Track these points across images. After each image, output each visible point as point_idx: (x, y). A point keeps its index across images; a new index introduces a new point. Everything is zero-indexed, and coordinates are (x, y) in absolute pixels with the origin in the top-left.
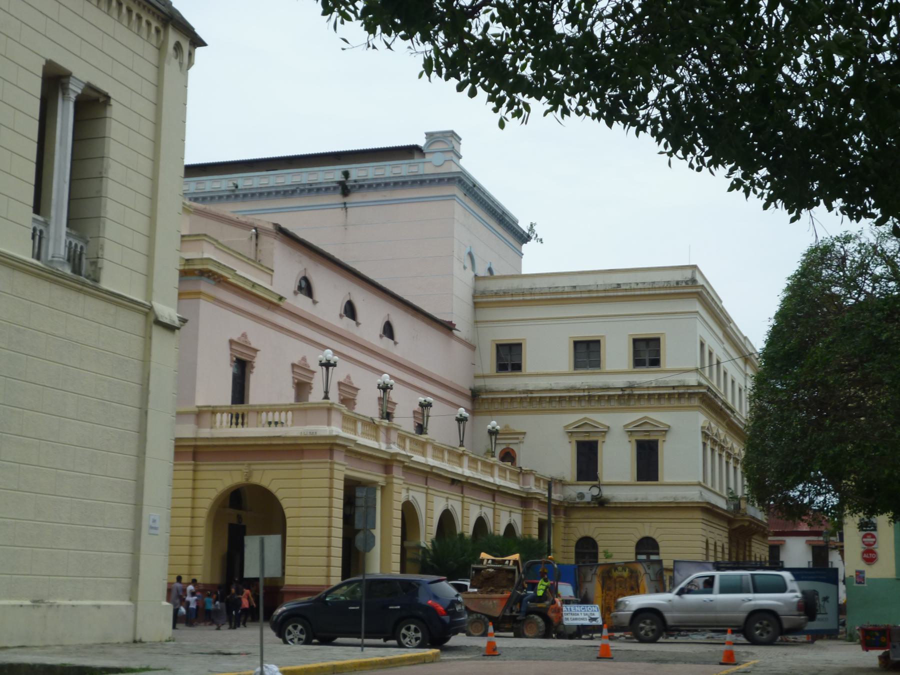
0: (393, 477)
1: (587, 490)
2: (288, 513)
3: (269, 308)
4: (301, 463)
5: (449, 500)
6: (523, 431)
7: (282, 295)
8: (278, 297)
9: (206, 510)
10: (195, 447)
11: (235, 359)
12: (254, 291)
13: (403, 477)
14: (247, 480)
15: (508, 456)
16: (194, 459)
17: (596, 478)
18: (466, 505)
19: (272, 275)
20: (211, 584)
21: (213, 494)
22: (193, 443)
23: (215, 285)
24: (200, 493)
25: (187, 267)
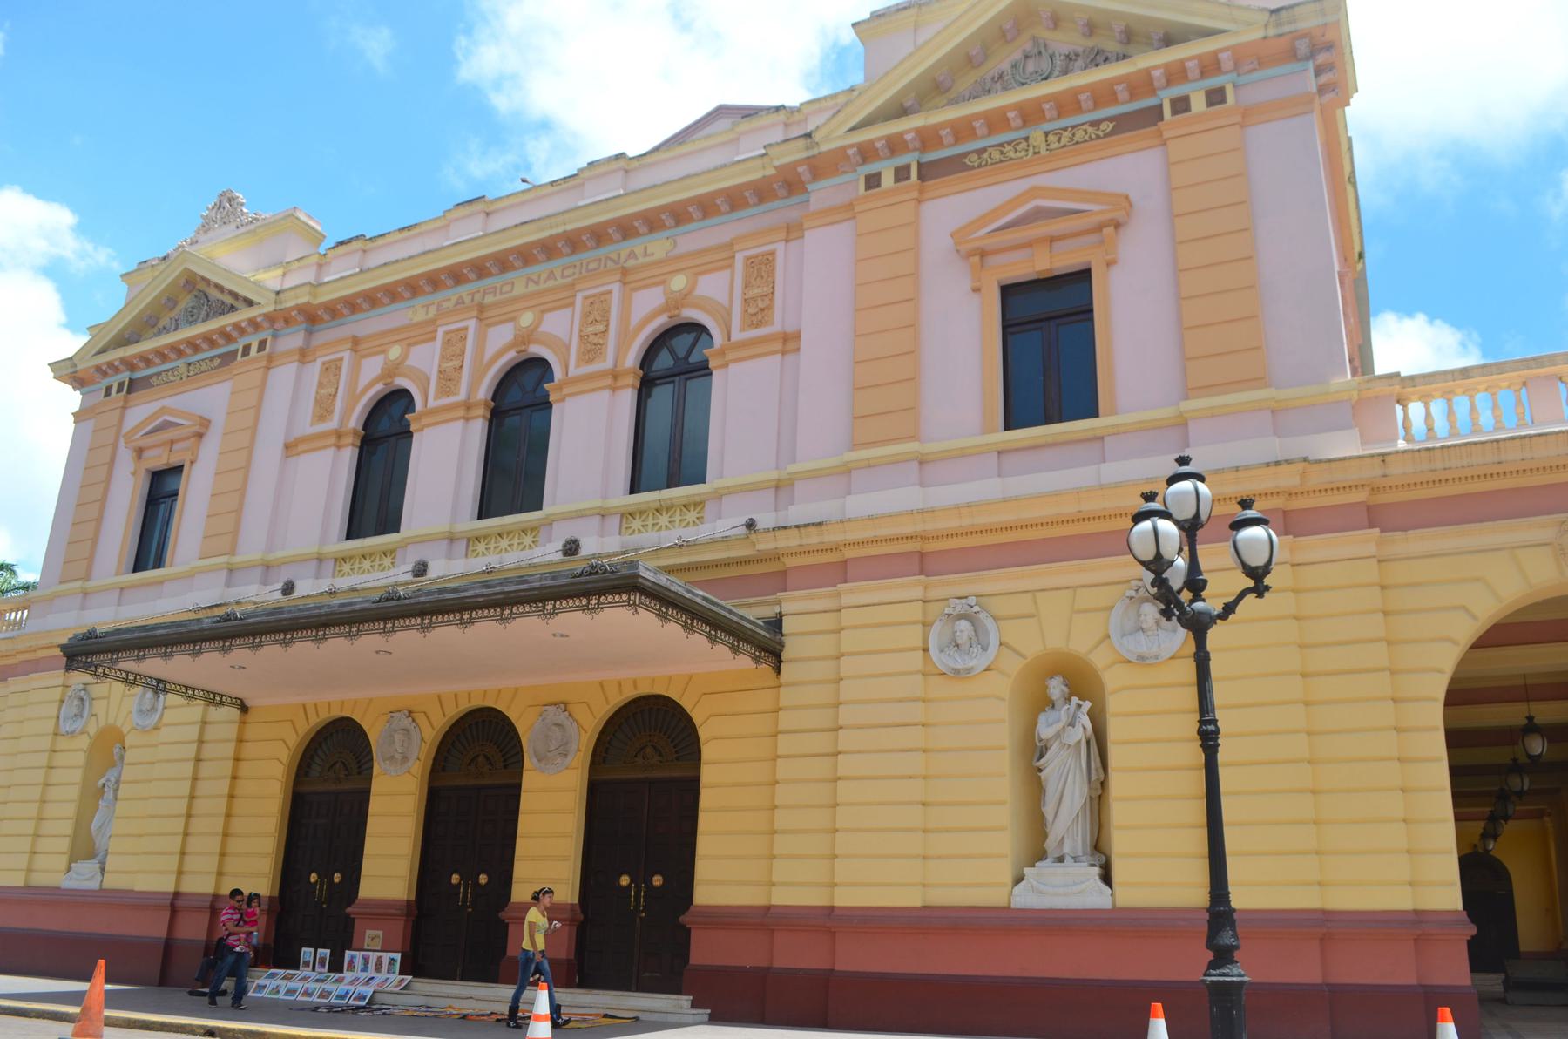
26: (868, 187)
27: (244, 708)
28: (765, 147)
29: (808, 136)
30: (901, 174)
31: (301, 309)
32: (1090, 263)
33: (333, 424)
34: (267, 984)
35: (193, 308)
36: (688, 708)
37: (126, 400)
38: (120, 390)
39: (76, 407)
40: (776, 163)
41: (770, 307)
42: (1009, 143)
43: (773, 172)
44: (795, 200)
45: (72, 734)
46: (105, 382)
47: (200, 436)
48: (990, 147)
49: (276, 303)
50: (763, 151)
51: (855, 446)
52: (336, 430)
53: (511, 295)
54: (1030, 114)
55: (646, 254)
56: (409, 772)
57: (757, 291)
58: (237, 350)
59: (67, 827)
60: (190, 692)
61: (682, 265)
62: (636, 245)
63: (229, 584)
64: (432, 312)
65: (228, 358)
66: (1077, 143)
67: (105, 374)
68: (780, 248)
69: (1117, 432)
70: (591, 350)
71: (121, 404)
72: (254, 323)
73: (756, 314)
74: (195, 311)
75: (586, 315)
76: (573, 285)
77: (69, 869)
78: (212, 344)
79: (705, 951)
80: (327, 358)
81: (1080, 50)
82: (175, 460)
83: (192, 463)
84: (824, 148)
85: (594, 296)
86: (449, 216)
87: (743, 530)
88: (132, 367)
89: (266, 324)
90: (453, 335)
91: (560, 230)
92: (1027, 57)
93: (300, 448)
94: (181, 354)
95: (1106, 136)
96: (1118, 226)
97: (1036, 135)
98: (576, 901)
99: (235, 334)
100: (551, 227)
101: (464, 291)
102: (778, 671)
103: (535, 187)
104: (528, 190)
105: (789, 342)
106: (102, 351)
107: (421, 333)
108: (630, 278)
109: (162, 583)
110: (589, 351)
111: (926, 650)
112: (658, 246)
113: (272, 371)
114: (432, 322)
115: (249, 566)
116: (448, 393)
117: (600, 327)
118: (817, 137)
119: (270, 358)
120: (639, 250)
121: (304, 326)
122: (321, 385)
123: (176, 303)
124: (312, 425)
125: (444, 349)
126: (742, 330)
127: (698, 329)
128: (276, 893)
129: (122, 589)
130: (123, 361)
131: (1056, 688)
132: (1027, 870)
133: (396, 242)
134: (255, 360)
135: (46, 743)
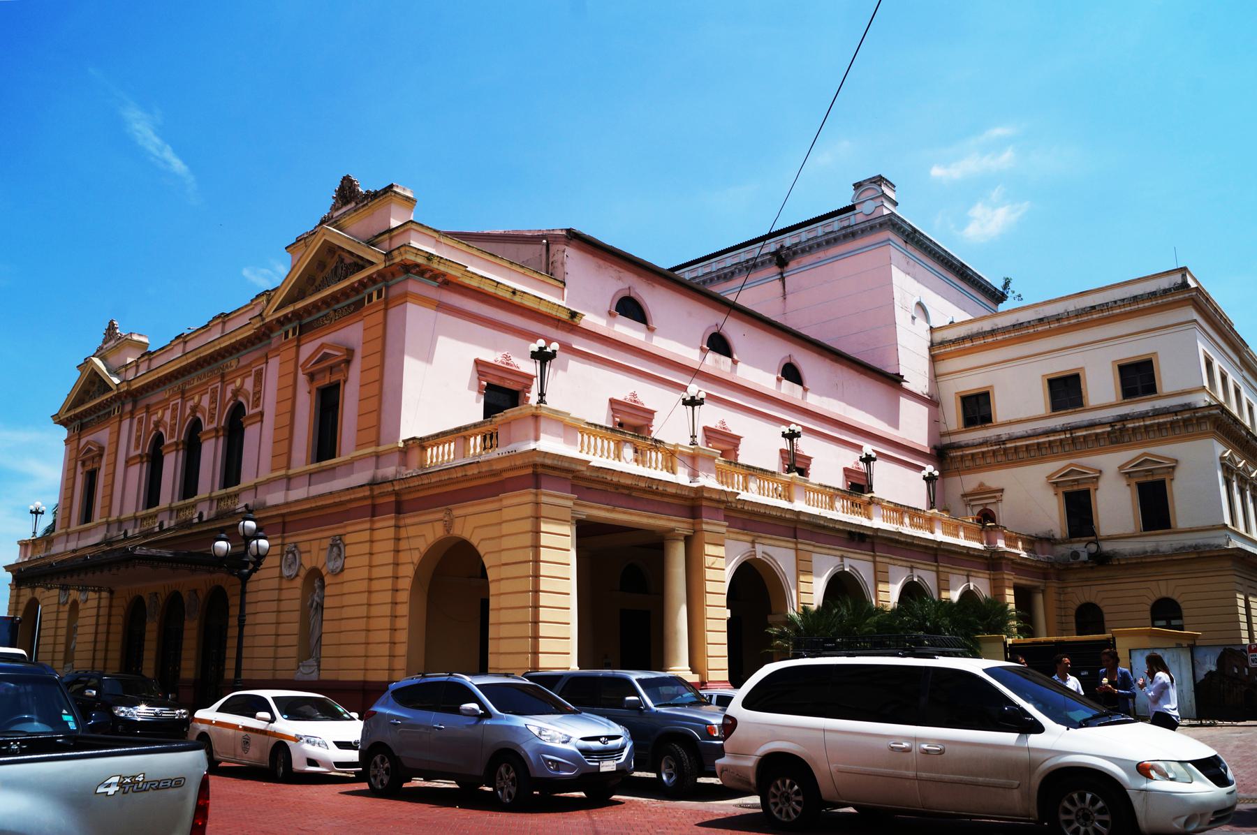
0: (702, 522)
1: (1082, 548)
3: (557, 327)
5: (845, 559)
6: (1001, 487)
11: (485, 383)
13: (727, 524)
14: (448, 531)
15: (986, 517)
17: (1093, 533)
18: (941, 574)
21: (416, 557)
25: (388, 264)
26: (285, 339)
27: (111, 592)
28: (250, 319)
30: (294, 330)
32: (340, 380)
33: (139, 452)
36: (226, 589)
39: (65, 436)
40: (255, 327)
41: (260, 397)
44: (266, 342)
45: (65, 604)
46: (72, 426)
47: (101, 456)
48: (321, 317)
49: (118, 389)
51: (273, 470)
53: (195, 384)
57: (257, 389)
59: (62, 648)
60: (81, 588)
61: (238, 374)
62: (227, 361)
63: (108, 530)
67: (72, 422)
68: (264, 366)
70: (212, 417)
71: (77, 437)
75: (211, 398)
77: (64, 668)
78: (104, 408)
80: (139, 416)
82: (96, 466)
83: (99, 469)
84: (267, 320)
86: (174, 343)
87: (244, 509)
88: (81, 419)
90: (175, 406)
92: (336, 267)
94: (95, 413)
99: (109, 404)
100: (196, 355)
101: (179, 382)
105: (261, 414)
106: (69, 410)
107: (164, 404)
108: (228, 378)
109: (90, 529)
110: (211, 417)
111: (281, 566)
112: (232, 363)
113: (123, 422)
114: (168, 399)
115: (114, 522)
116: (173, 437)
117: (213, 406)
118: (264, 314)
119: (121, 416)
120: (229, 364)
121: (131, 399)
122: (137, 431)
126: (252, 409)
127: (241, 404)
131: (317, 583)
132: (300, 664)
135: (55, 608)
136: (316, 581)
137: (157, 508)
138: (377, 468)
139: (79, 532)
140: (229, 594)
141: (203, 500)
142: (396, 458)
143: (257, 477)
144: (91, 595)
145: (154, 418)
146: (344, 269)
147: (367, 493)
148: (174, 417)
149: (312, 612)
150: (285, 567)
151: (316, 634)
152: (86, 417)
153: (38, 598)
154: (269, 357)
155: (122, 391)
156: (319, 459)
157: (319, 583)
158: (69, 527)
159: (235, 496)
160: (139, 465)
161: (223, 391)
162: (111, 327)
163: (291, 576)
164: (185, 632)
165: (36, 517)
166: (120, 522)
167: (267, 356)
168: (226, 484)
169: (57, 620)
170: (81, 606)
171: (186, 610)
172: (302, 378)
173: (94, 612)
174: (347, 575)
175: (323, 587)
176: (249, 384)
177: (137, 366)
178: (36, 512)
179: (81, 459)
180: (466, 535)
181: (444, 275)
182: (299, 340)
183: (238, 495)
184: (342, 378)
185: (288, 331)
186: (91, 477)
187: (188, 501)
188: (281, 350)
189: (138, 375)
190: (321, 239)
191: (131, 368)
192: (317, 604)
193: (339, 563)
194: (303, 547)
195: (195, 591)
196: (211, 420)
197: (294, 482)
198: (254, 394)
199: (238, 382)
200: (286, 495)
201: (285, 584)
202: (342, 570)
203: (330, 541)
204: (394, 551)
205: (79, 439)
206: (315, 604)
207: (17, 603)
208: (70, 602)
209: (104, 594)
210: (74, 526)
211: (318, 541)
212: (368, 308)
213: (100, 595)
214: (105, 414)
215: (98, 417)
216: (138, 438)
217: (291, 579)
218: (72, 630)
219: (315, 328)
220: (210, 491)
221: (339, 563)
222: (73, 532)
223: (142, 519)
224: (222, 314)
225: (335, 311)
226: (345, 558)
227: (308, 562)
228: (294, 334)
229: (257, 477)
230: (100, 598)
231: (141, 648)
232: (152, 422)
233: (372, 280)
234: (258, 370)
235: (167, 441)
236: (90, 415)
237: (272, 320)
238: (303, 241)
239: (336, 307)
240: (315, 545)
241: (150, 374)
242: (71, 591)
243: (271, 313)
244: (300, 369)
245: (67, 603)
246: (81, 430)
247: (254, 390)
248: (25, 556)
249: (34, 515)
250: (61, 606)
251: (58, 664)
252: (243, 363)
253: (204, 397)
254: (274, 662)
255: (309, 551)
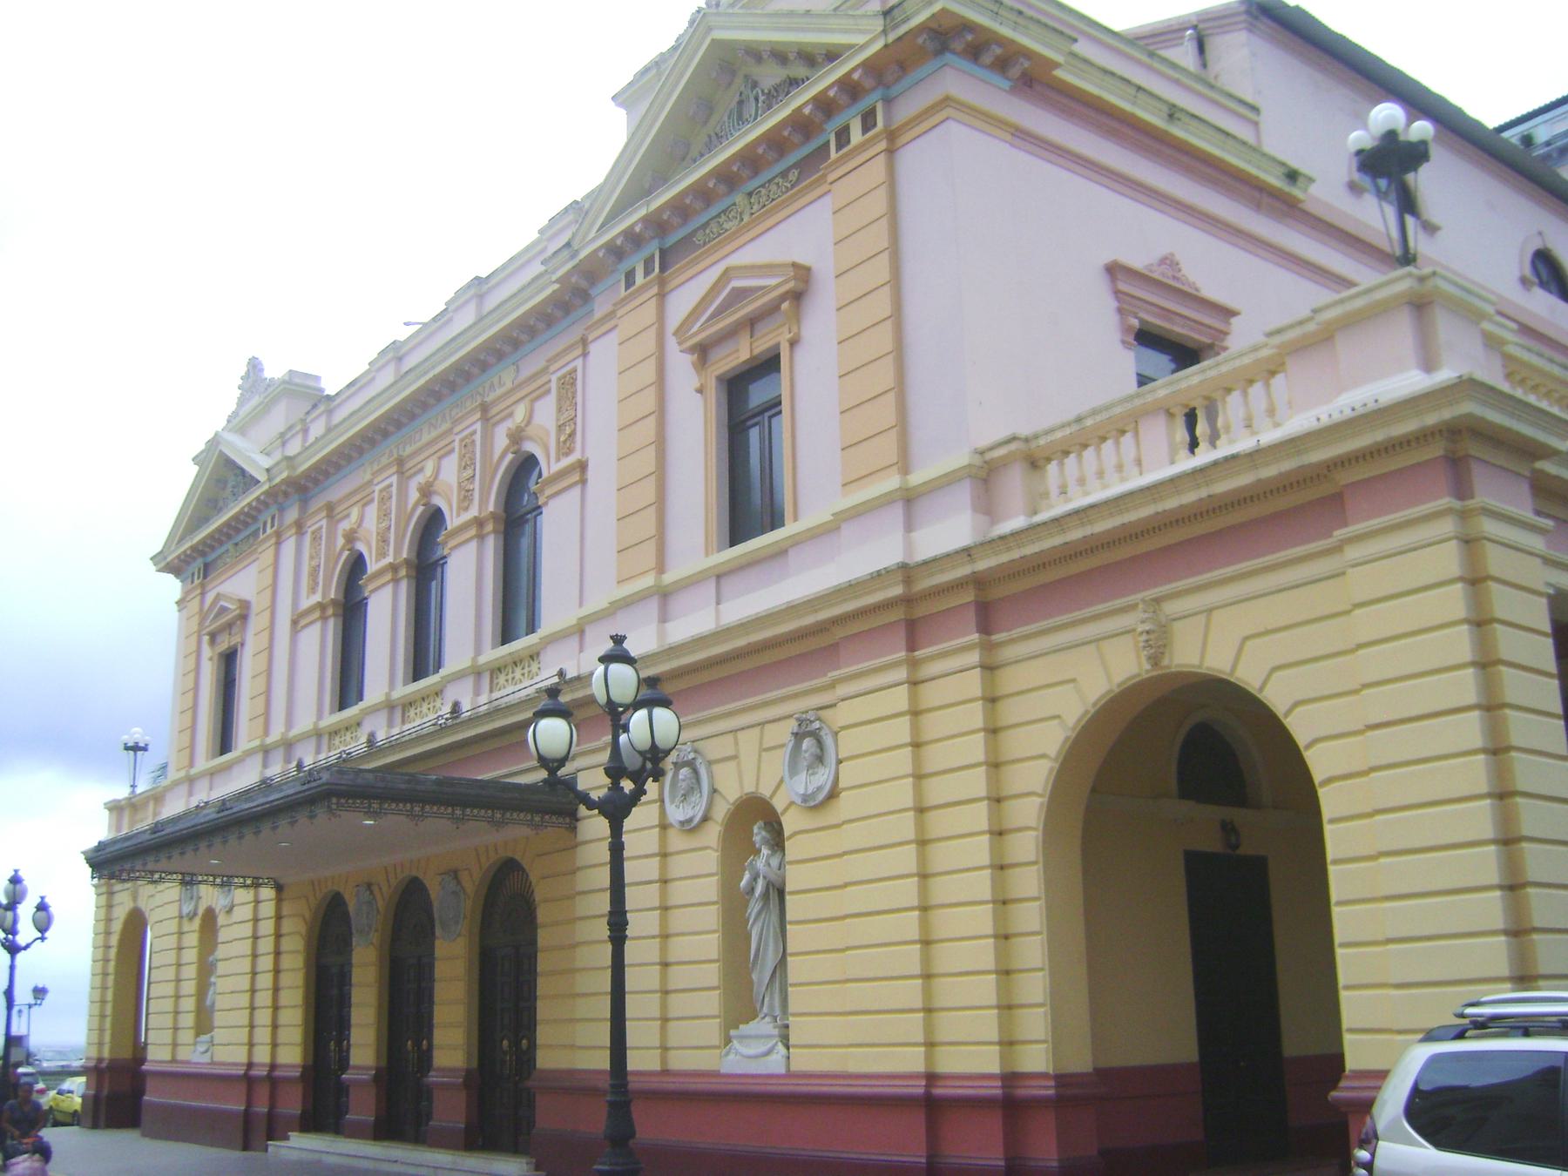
2: (1319, 763)
4: (1338, 548)
7: (1294, 164)
8: (1280, 171)
9: (1038, 800)
10: (979, 582)
12: (1177, 131)
14: (1155, 660)
16: (985, 627)
19: (1256, 124)
20: (1102, 1074)
22: (964, 571)
23: (1014, 91)
24: (1015, 744)
25: (891, 37)
26: (627, 288)
27: (279, 888)
29: (568, 245)
31: (286, 482)
32: (777, 346)
33: (317, 598)
34: (301, 1145)
35: (234, 487)
37: (203, 586)
38: (198, 578)
39: (177, 595)
40: (554, 278)
41: (572, 435)
42: (724, 212)
43: (556, 286)
47: (244, 617)
48: (711, 219)
49: (270, 480)
50: (543, 268)
52: (319, 602)
54: (703, 194)
55: (501, 384)
56: (372, 944)
57: (565, 416)
58: (259, 529)
59: (189, 1004)
63: (265, 765)
64: (376, 467)
65: (255, 534)
66: (773, 200)
68: (579, 363)
69: (797, 541)
70: (466, 498)
71: (199, 591)
72: (262, 505)
73: (565, 442)
74: (236, 490)
75: (462, 457)
76: (450, 430)
78: (246, 524)
79: (548, 1116)
81: (778, 81)
82: (236, 640)
83: (242, 645)
84: (583, 255)
85: (466, 437)
88: (203, 554)
89: (270, 501)
90: (384, 493)
91: (430, 375)
92: (741, 103)
93: (303, 622)
94: (229, 537)
95: (793, 186)
96: (797, 297)
97: (739, 198)
98: (475, 1064)
99: (254, 513)
100: (425, 373)
102: (574, 829)
103: (425, 325)
104: (418, 332)
105: (582, 466)
106: (182, 539)
110: (465, 497)
111: (662, 801)
112: (506, 377)
115: (276, 746)
117: (469, 472)
118: (575, 246)
119: (278, 534)
120: (496, 380)
122: (312, 558)
123: (226, 483)
124: (308, 598)
125: (379, 510)
126: (558, 460)
128: (310, 1062)
129: (212, 774)
130: (193, 548)
131: (759, 833)
132: (733, 1032)
133: (349, 398)
134: (269, 537)
135: (172, 926)
136: (756, 830)
137: (361, 705)
138: (909, 527)
139: (212, 774)
140: (533, 878)
141: (459, 676)
142: (963, 494)
143: (581, 605)
144: (242, 895)
145: (345, 525)
146: (762, 98)
147: (897, 590)
148: (384, 514)
149: (754, 907)
150: (672, 802)
151: (770, 961)
152: (213, 548)
153: (144, 909)
154: (590, 338)
155: (277, 480)
156: (736, 535)
157: (764, 833)
158: (192, 764)
159: (532, 657)
160: (318, 626)
161: (488, 438)
162: (254, 366)
163: (690, 820)
164: (437, 964)
165: (135, 755)
166: (288, 745)
167: (584, 342)
168: (506, 634)
169: (180, 949)
170: (221, 920)
171: (436, 916)
172: (681, 366)
173: (247, 930)
174: (847, 805)
175: (777, 840)
176: (546, 413)
177: (305, 431)
178: (136, 748)
179: (208, 630)
180: (1217, 662)
181: (1028, 54)
182: (662, 282)
183: (538, 654)
184: (784, 338)
185: (634, 268)
186: (229, 660)
187: (423, 683)
188: (619, 314)
189: (307, 444)
190: (704, 39)
191: (293, 436)
192: (769, 885)
193: (823, 777)
194: (713, 749)
195: (455, 874)
196: (466, 504)
197: (679, 602)
198: (560, 428)
199: (520, 413)
200: (661, 634)
201: (677, 841)
202: (833, 794)
203: (792, 725)
204: (985, 730)
205: (203, 594)
206: (760, 888)
207: (109, 920)
208: (201, 911)
209: (267, 893)
210: (203, 763)
211: (757, 730)
212: (841, 161)
213: (256, 895)
214: (248, 537)
215: (236, 544)
216: (314, 572)
217: (691, 827)
218: (206, 970)
219: (700, 247)
220: (472, 655)
221: (823, 777)
222: (202, 775)
223: (330, 734)
224: (477, 278)
225: (750, 194)
226: (839, 762)
227: (732, 786)
228: (647, 273)
229: (581, 605)
230: (257, 902)
231: (344, 1002)
232: (340, 532)
233: (850, 89)
234: (564, 376)
235: (372, 566)
236: (221, 543)
237: (596, 251)
238: (654, 71)
239: (752, 185)
240: (749, 740)
241: (333, 434)
242: (203, 888)
243: (592, 234)
244: (672, 344)
245: (195, 914)
246: (205, 577)
247: (558, 420)
248: (119, 828)
249: (131, 753)
250: (185, 920)
251: (186, 1036)
252: (526, 373)
253: (445, 462)
254: (663, 1029)
255: (735, 757)
